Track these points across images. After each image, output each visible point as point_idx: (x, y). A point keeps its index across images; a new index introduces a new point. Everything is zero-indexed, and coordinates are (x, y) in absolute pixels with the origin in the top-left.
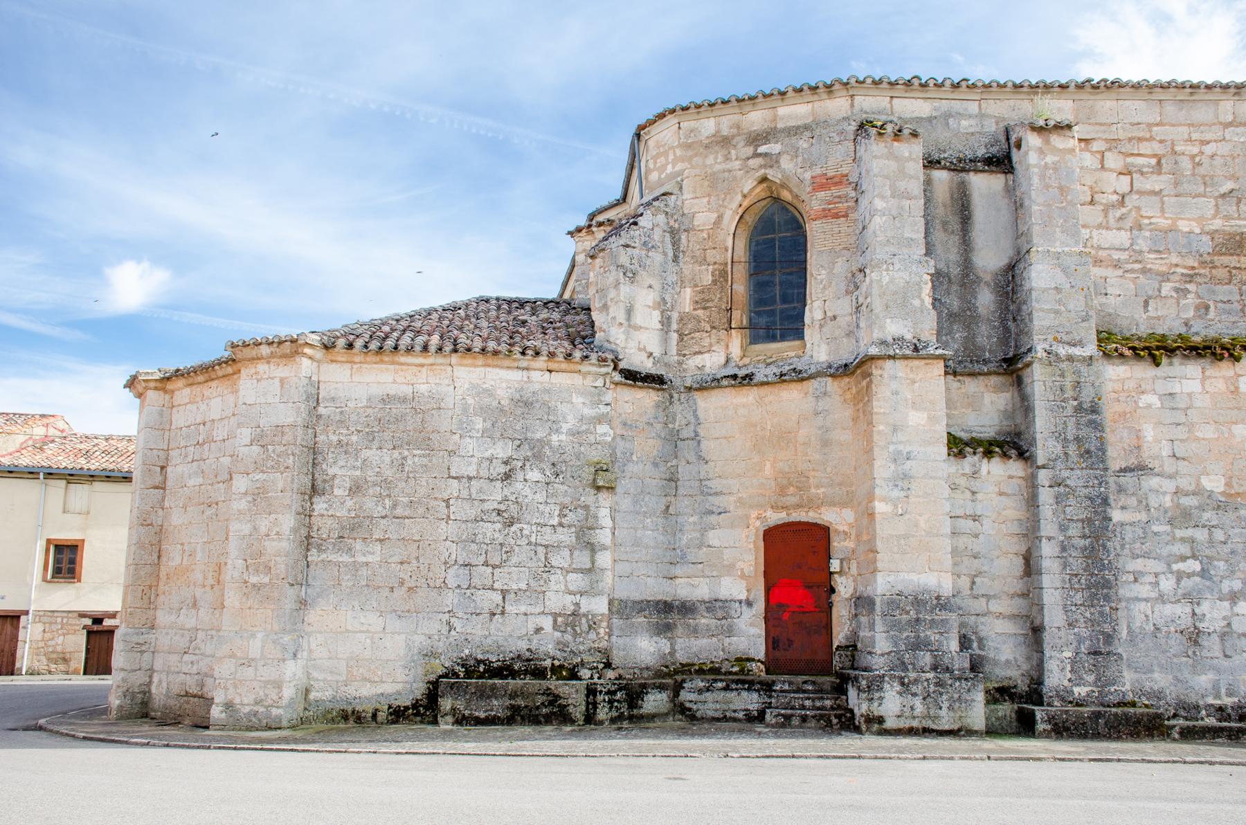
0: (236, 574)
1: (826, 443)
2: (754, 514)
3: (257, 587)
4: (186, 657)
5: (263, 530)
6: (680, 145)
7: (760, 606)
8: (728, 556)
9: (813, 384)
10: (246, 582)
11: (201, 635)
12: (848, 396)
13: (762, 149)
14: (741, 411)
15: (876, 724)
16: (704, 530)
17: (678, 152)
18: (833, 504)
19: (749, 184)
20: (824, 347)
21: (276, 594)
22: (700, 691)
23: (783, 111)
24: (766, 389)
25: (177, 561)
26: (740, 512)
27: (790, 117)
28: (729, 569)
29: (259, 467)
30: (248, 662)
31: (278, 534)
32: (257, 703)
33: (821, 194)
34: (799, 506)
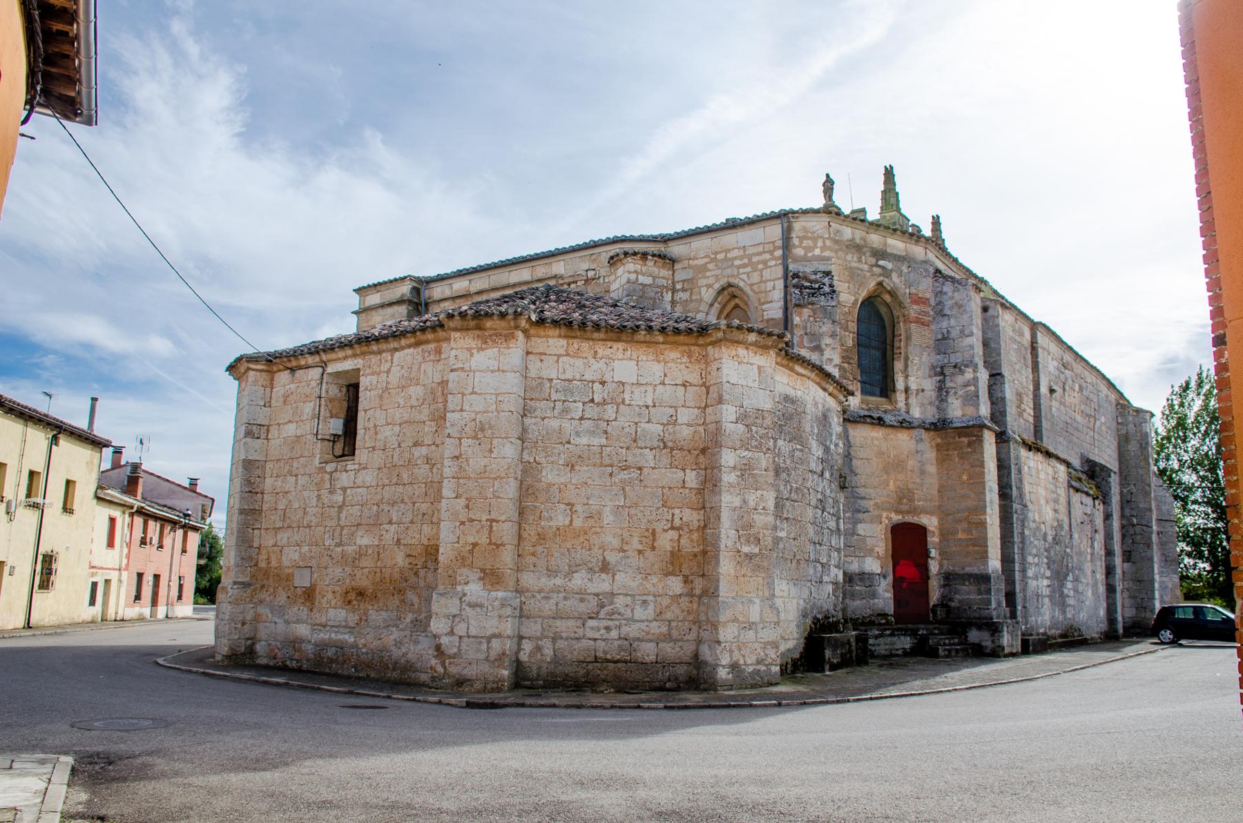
0: (730, 544)
1: (923, 472)
2: (884, 515)
3: (750, 557)
4: (591, 623)
5: (752, 504)
6: (829, 238)
7: (890, 578)
8: (869, 542)
9: (916, 432)
10: (739, 551)
11: (620, 602)
12: (933, 444)
13: (881, 263)
14: (875, 442)
15: (995, 654)
16: (855, 522)
17: (828, 243)
18: (927, 513)
19: (872, 285)
20: (918, 409)
21: (765, 564)
22: (876, 637)
23: (890, 241)
24: (889, 431)
25: (561, 520)
26: (876, 513)
27: (894, 247)
28: (870, 552)
29: (745, 445)
30: (751, 626)
31: (764, 508)
32: (759, 662)
33: (915, 307)
34: (909, 512)
